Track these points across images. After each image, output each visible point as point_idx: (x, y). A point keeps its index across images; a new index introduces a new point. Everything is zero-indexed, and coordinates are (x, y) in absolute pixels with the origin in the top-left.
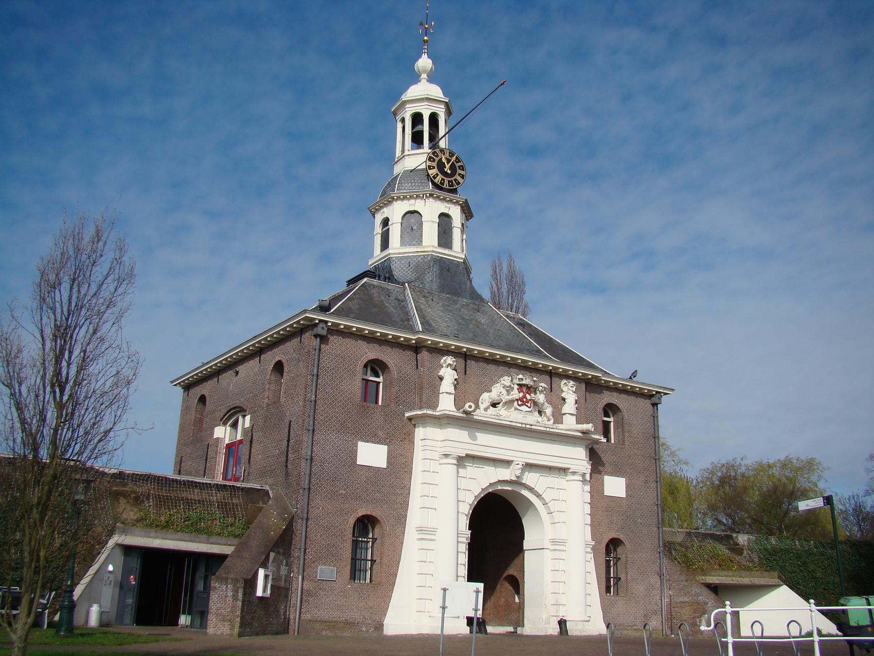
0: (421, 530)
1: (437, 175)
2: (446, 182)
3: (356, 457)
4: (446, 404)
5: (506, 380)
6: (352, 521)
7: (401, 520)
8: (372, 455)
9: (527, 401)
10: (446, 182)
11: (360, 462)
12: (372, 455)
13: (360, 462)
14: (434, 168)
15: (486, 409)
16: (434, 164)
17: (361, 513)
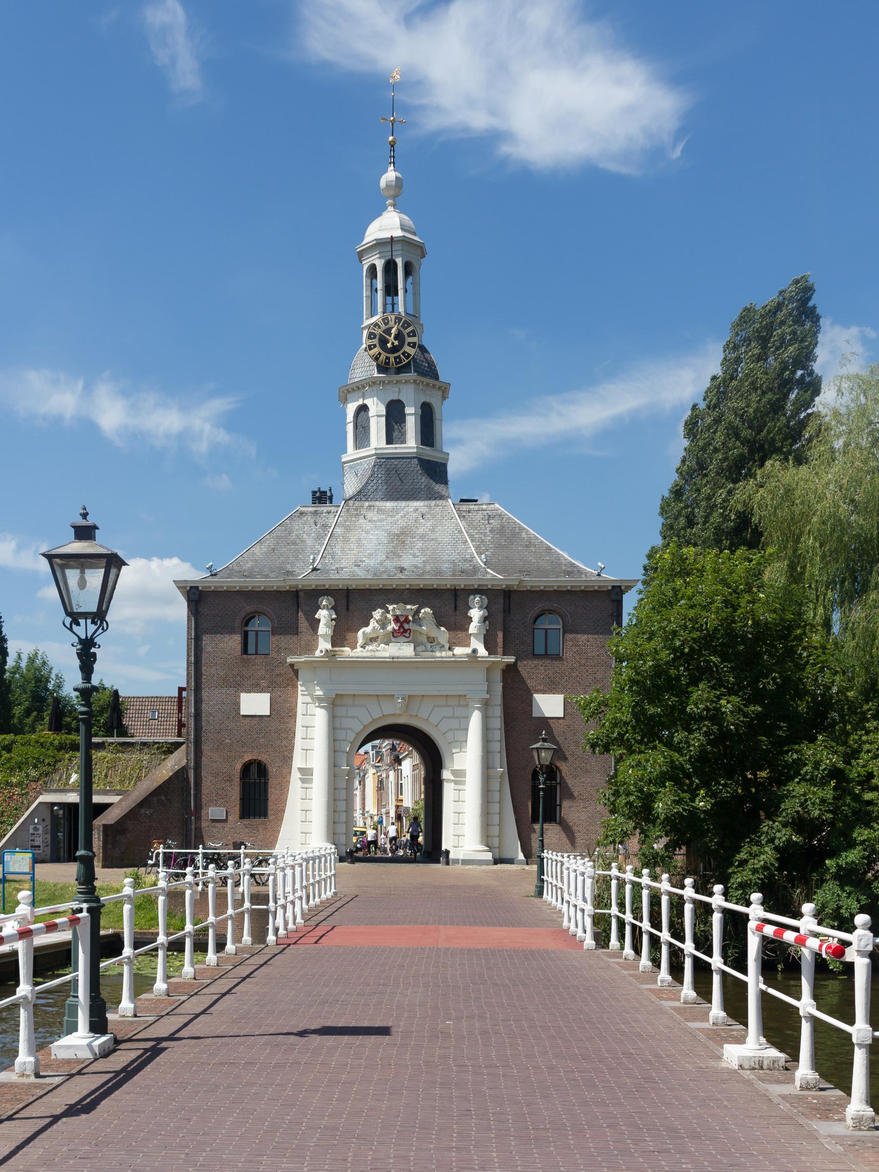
0: (300, 770)
1: (380, 354)
2: (392, 360)
3: (239, 708)
4: (324, 645)
5: (377, 614)
6: (238, 766)
7: (287, 759)
8: (255, 704)
9: (405, 631)
10: (392, 360)
11: (243, 712)
12: (255, 704)
13: (243, 712)
14: (375, 346)
15: (363, 647)
16: (376, 341)
17: (247, 758)
